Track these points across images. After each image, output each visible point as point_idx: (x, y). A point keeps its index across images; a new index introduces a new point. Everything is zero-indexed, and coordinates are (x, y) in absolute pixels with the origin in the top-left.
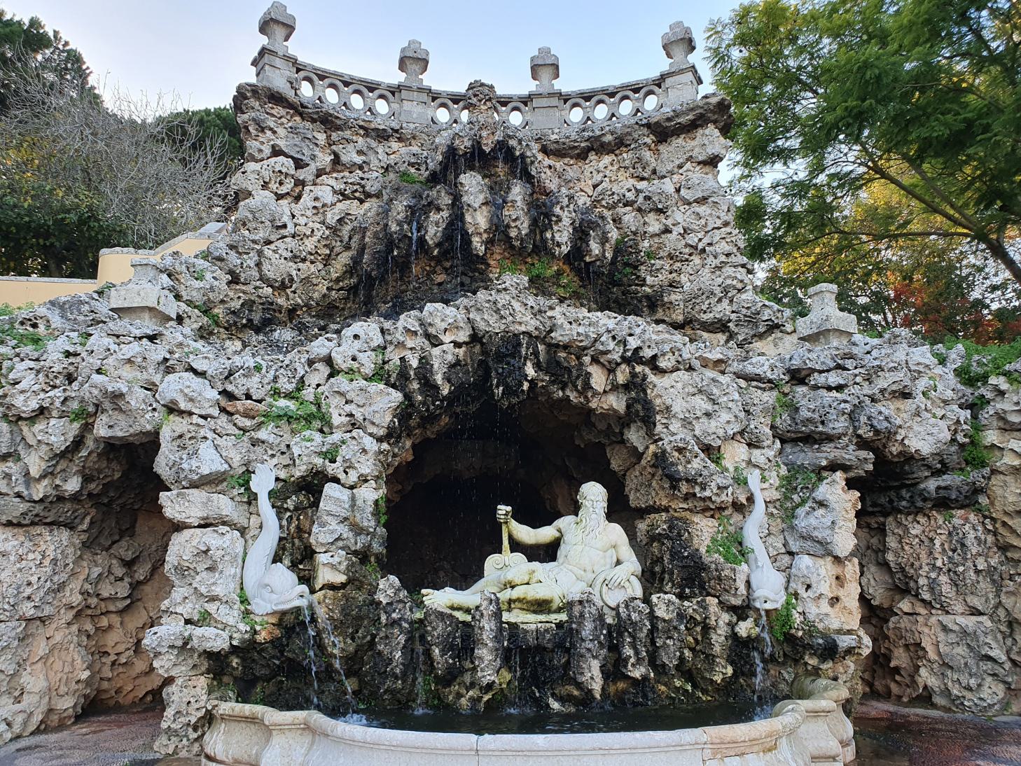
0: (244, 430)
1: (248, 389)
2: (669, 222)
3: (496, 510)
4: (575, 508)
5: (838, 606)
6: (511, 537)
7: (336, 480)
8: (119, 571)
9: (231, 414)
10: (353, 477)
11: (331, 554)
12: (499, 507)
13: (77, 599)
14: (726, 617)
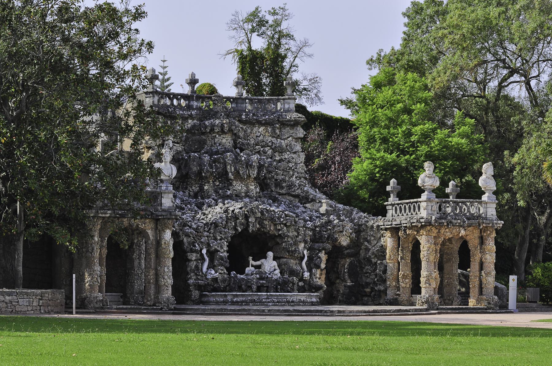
2: (283, 157)
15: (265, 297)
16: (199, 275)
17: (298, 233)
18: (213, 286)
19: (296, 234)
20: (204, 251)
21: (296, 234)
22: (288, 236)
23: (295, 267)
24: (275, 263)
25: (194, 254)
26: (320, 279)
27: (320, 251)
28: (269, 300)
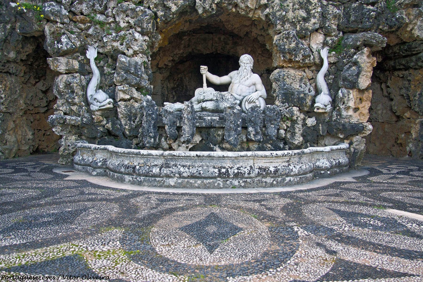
0: (82, 30)
1: (81, 10)
3: (199, 68)
4: (237, 67)
5: (358, 113)
6: (207, 80)
7: (124, 54)
8: (41, 95)
9: (75, 22)
10: (131, 52)
11: (123, 86)
12: (201, 66)
13: (23, 106)
14: (302, 116)
15: (160, 162)
16: (75, 104)
17: (308, 12)
18: (104, 126)
19: (304, 15)
20: (92, 54)
21: (304, 15)
22: (284, 20)
23: (296, 86)
24: (256, 78)
25: (63, 60)
26: (356, 109)
27: (357, 49)
28: (165, 171)
